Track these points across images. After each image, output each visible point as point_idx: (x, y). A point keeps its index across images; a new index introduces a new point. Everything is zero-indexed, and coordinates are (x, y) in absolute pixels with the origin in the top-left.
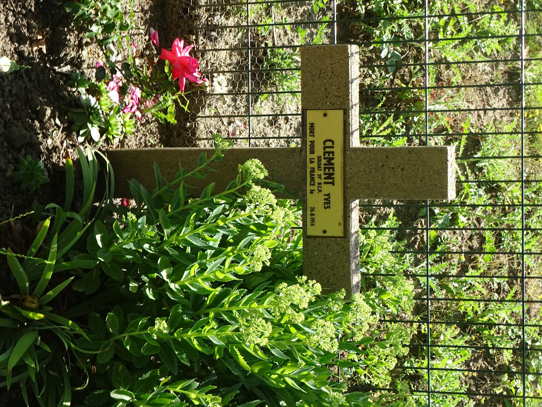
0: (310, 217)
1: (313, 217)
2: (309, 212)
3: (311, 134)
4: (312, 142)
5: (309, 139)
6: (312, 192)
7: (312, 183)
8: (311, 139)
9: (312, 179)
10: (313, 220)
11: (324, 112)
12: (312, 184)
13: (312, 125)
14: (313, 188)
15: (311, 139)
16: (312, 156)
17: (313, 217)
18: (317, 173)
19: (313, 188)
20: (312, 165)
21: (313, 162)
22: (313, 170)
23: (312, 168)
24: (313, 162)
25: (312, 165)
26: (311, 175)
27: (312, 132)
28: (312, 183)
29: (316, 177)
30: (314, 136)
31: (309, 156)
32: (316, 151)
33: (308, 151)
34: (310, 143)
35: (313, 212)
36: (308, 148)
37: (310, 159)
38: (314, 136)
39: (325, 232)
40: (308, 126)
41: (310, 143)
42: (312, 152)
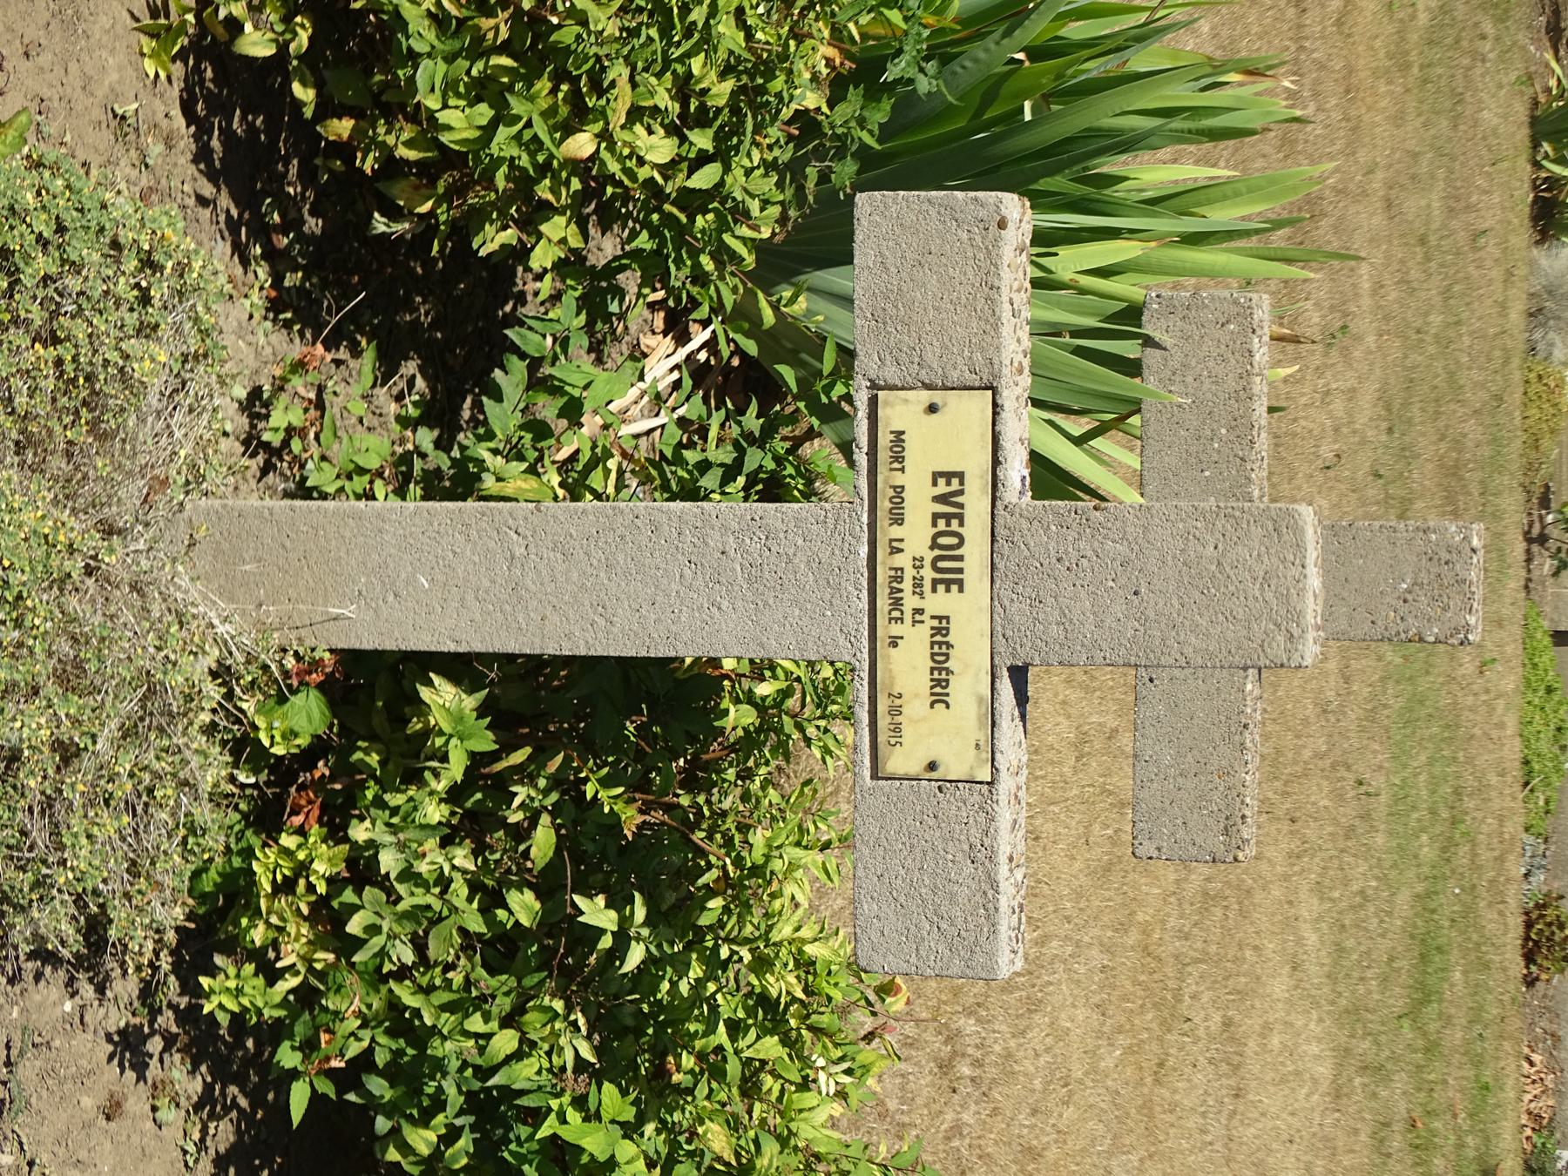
0: (889, 719)
2: (882, 707)
3: (896, 465)
4: (899, 490)
7: (896, 614)
9: (897, 603)
10: (897, 729)
11: (937, 397)
12: (896, 619)
13: (899, 435)
14: (896, 629)
15: (899, 479)
16: (896, 531)
19: (896, 629)
23: (896, 569)
27: (898, 458)
28: (896, 614)
31: (888, 531)
32: (906, 517)
34: (891, 493)
36: (884, 505)
37: (891, 541)
38: (903, 470)
39: (932, 766)
40: (884, 439)
41: (891, 493)
42: (899, 520)
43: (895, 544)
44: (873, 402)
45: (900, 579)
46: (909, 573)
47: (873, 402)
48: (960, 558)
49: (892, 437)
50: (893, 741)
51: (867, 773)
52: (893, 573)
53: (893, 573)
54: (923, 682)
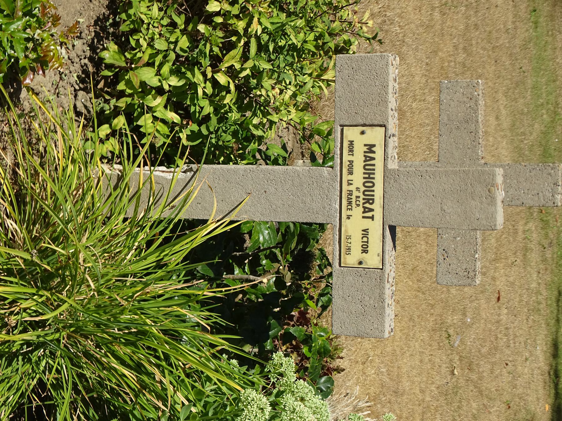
4: (351, 162)
5: (346, 157)
6: (348, 217)
7: (350, 207)
8: (351, 158)
9: (350, 203)
10: (349, 249)
12: (350, 209)
13: (351, 143)
15: (351, 158)
16: (350, 177)
17: (349, 245)
19: (349, 213)
21: (352, 184)
22: (350, 193)
23: (350, 191)
24: (352, 184)
26: (349, 199)
27: (351, 150)
28: (350, 207)
29: (354, 200)
30: (353, 155)
31: (345, 177)
33: (345, 171)
34: (349, 163)
37: (348, 180)
38: (353, 155)
40: (346, 144)
41: (349, 163)
42: (351, 173)
43: (350, 182)
44: (342, 131)
45: (351, 195)
47: (342, 131)
49: (349, 143)
50: (347, 253)
51: (337, 264)
52: (349, 192)
53: (349, 192)
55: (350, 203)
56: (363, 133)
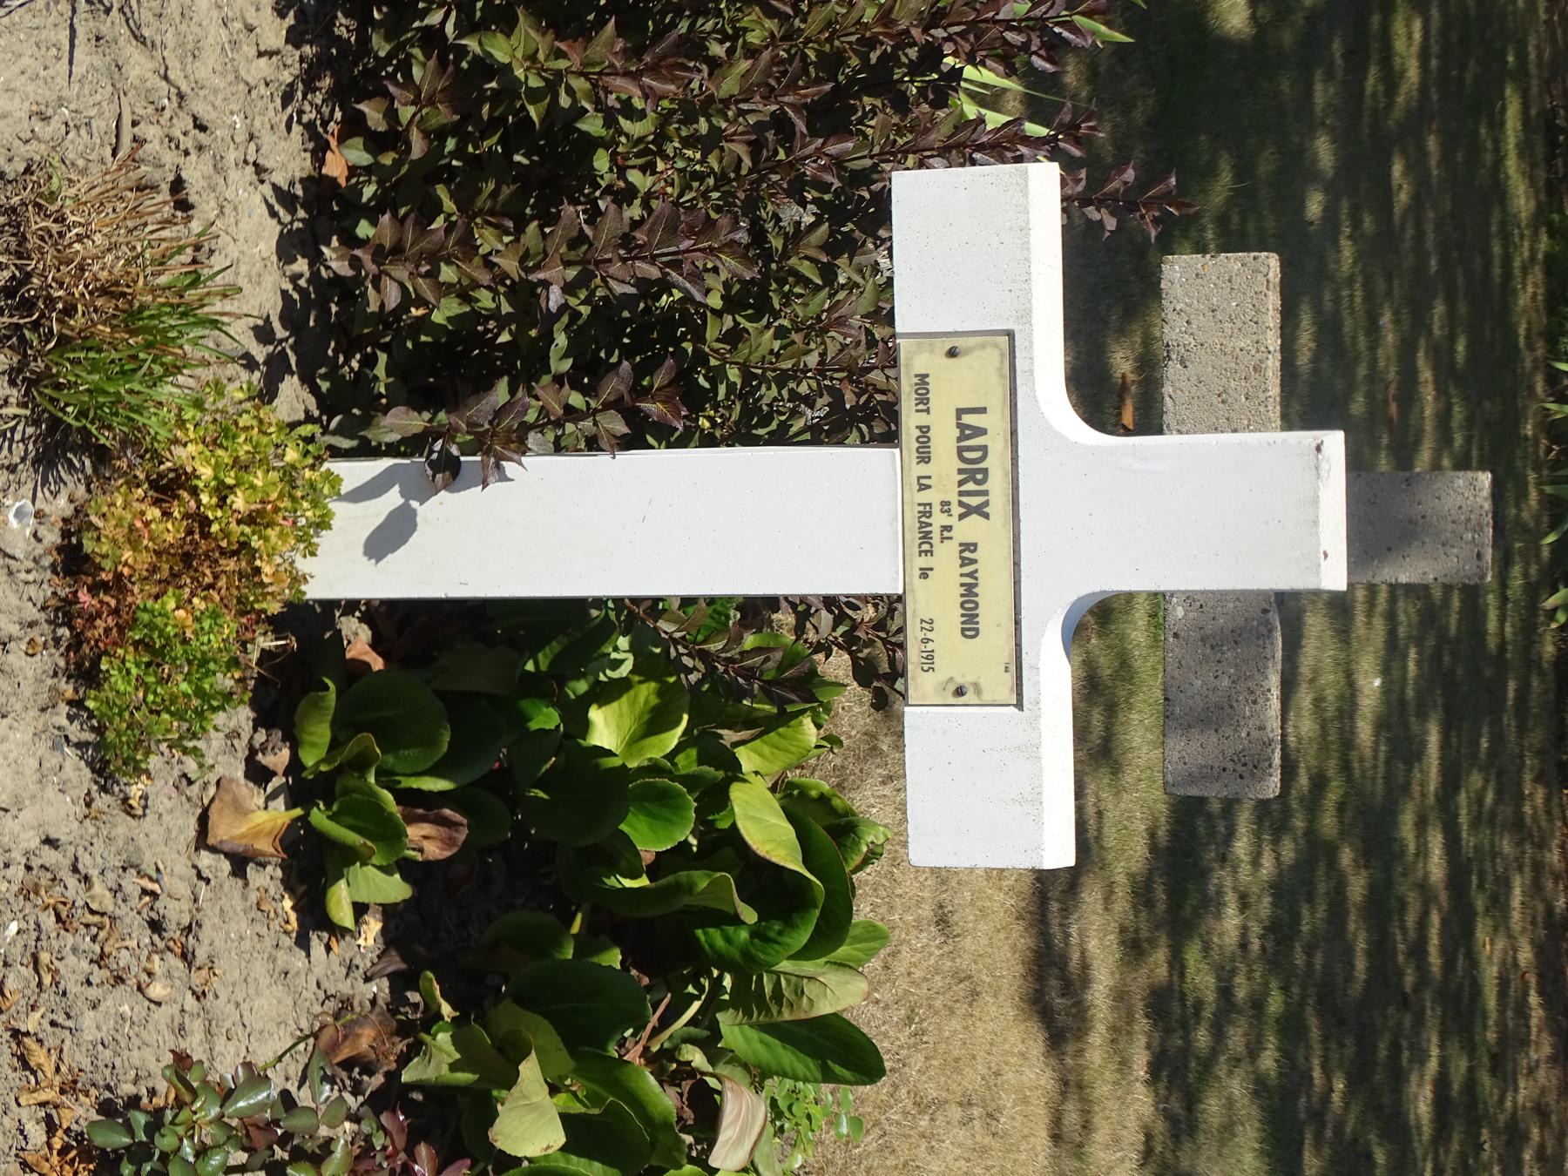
1: (930, 646)
3: (921, 407)
4: (924, 430)
6: (924, 573)
7: (926, 547)
8: (923, 419)
9: (926, 537)
10: (930, 657)
12: (926, 552)
14: (923, 562)
15: (923, 419)
17: (930, 646)
18: (938, 520)
19: (923, 562)
20: (925, 496)
21: (929, 487)
24: (929, 487)
25: (925, 496)
26: (923, 525)
27: (923, 400)
28: (926, 547)
30: (928, 411)
34: (918, 433)
35: (929, 635)
38: (928, 411)
41: (918, 433)
42: (924, 458)
45: (929, 514)
46: (936, 508)
48: (985, 493)
49: (916, 380)
54: (955, 616)
55: (926, 537)
56: (952, 353)
